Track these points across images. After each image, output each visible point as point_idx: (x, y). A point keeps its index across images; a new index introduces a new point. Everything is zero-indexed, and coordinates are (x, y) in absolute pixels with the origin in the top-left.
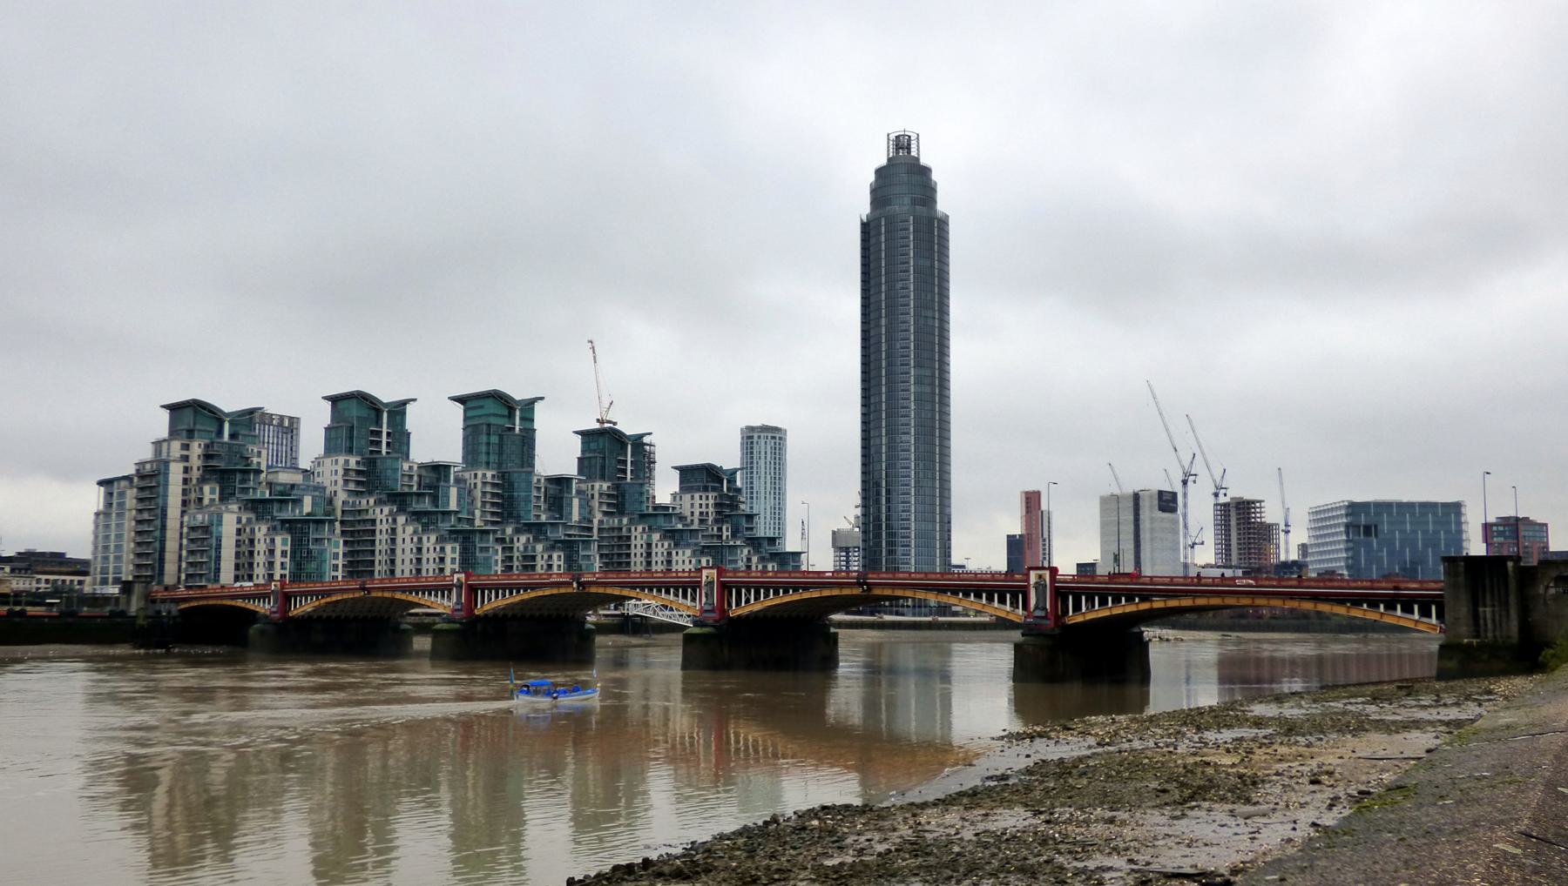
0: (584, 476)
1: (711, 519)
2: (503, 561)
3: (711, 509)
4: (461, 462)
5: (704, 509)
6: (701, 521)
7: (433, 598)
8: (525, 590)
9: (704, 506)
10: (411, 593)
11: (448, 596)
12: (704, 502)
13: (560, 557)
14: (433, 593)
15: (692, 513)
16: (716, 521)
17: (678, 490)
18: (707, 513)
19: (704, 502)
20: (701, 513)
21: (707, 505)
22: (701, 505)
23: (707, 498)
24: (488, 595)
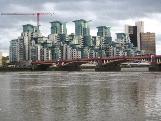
0: (77, 34)
1: (124, 44)
2: (61, 54)
3: (124, 42)
5: (122, 42)
6: (122, 45)
12: (122, 41)
13: (80, 52)
15: (120, 43)
16: (125, 45)
18: (123, 43)
19: (122, 41)
20: (122, 43)
21: (123, 41)
22: (122, 41)
23: (123, 40)
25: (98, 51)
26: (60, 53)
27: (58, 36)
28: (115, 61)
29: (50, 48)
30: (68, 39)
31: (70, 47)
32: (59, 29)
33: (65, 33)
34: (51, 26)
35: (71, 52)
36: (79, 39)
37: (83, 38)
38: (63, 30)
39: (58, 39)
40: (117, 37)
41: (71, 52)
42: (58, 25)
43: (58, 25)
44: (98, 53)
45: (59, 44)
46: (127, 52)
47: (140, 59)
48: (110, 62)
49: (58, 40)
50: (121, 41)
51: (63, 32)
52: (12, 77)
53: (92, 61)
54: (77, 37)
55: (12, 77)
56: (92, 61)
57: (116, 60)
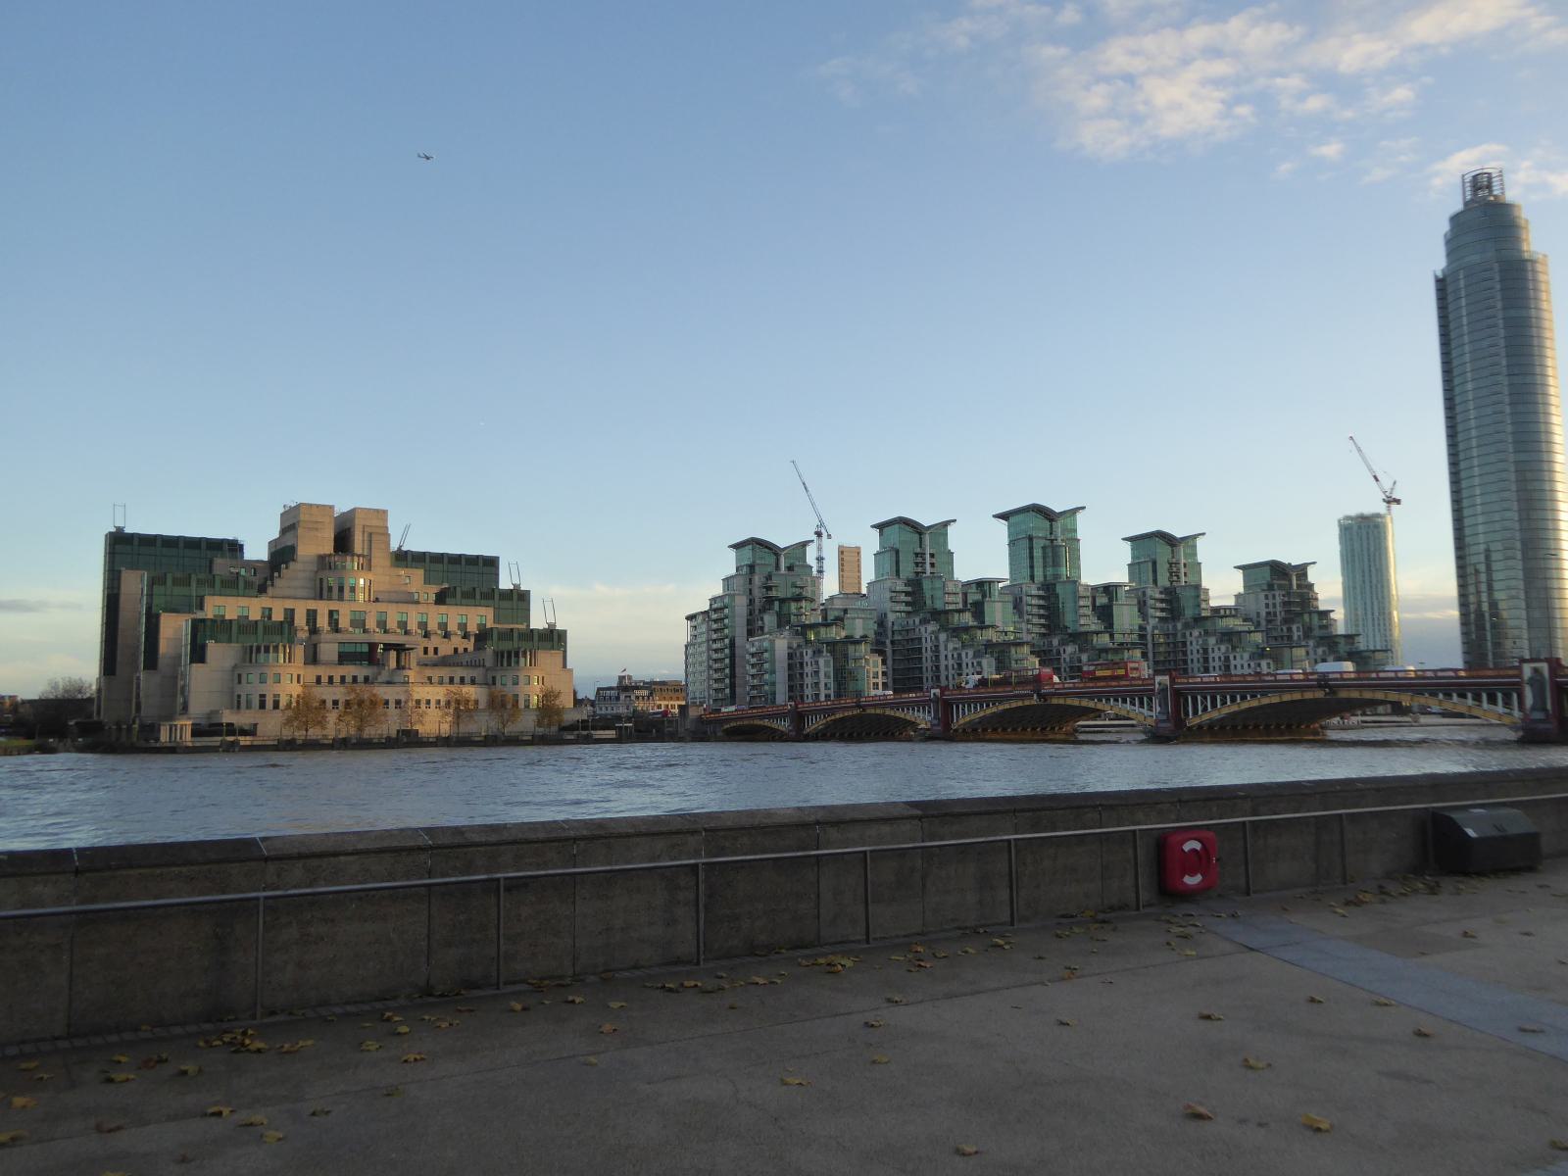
1: (1279, 618)
3: (1278, 609)
4: (1127, 581)
5: (1271, 609)
6: (1269, 622)
7: (1128, 706)
8: (1243, 698)
9: (1271, 606)
10: (1100, 700)
16: (1286, 621)
17: (1242, 590)
18: (1275, 613)
19: (1271, 602)
20: (1268, 613)
21: (1274, 605)
22: (1267, 605)
23: (1274, 597)
24: (1202, 703)
31: (1317, 646)
33: (1192, 580)
34: (1129, 561)
35: (1199, 656)
39: (1162, 610)
45: (1168, 629)
49: (1164, 614)
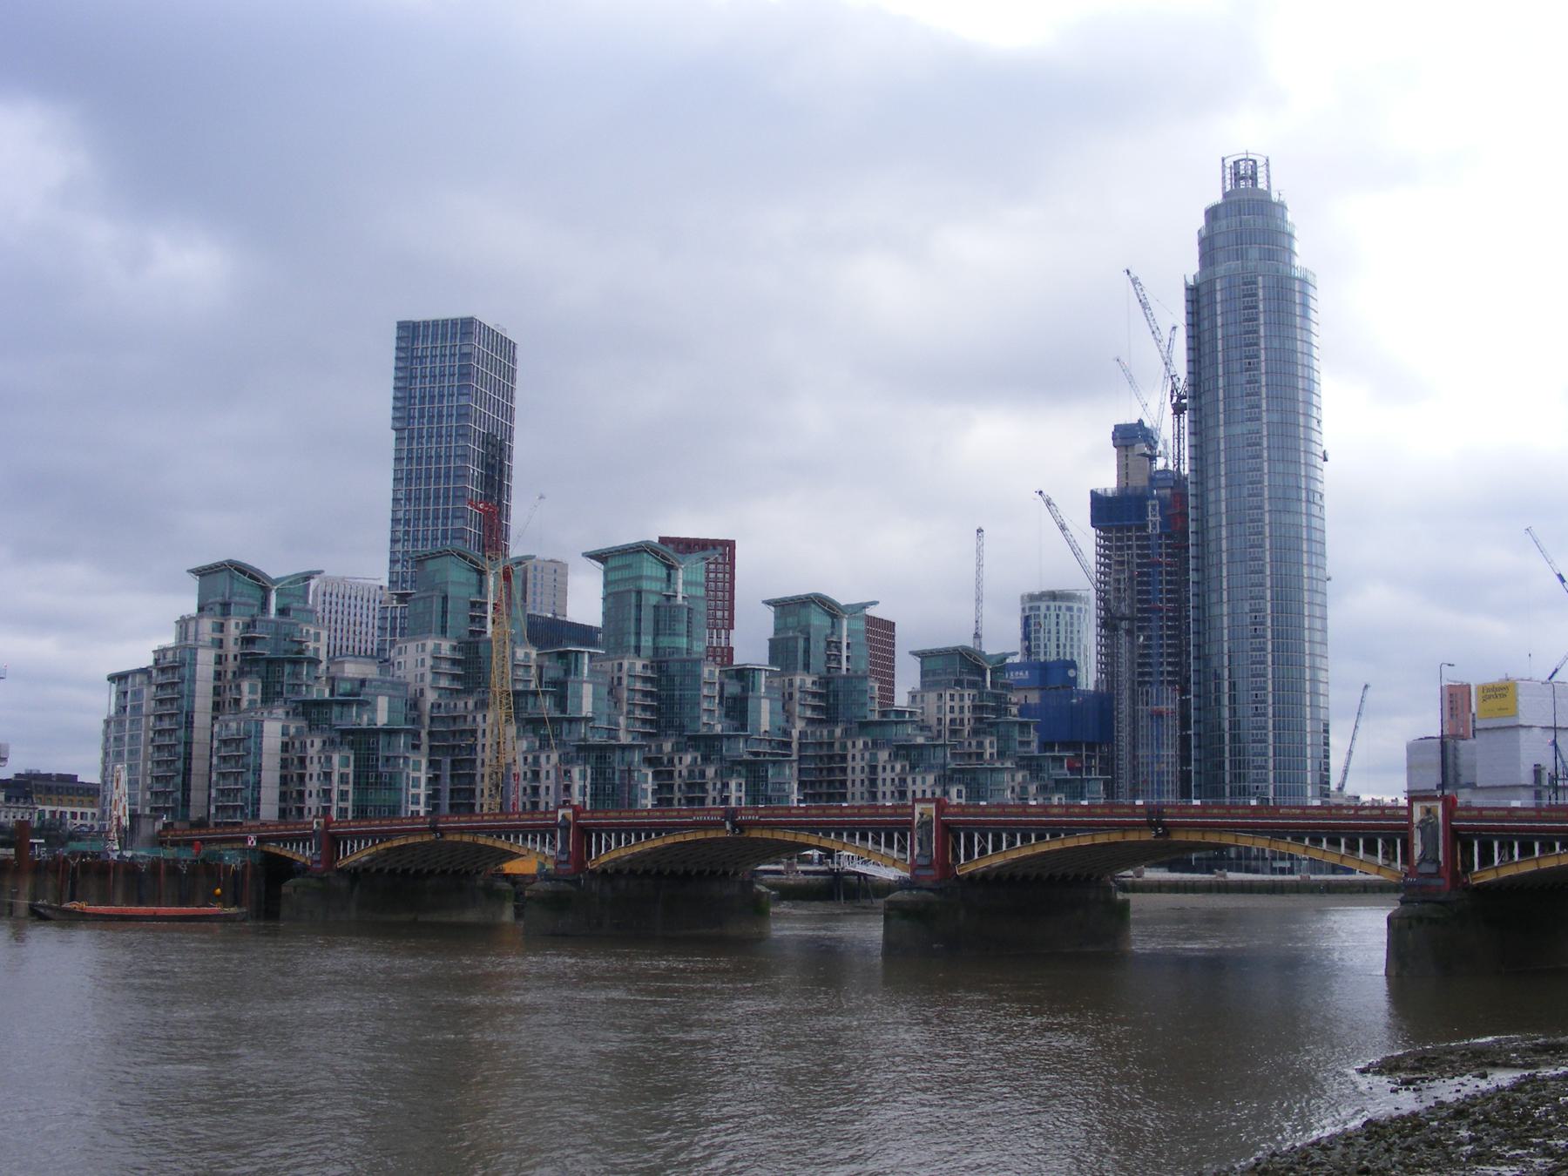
1: (967, 729)
2: (654, 792)
3: (967, 715)
5: (956, 715)
6: (954, 732)
9: (957, 709)
11: (550, 843)
14: (529, 837)
16: (975, 732)
17: (918, 686)
18: (962, 720)
19: (956, 704)
20: (952, 721)
21: (962, 708)
22: (952, 708)
24: (606, 840)
25: (959, 781)
26: (650, 785)
27: (649, 673)
28: (1071, 843)
29: (584, 750)
30: (716, 693)
32: (823, 644)
36: (791, 695)
37: (815, 689)
38: (845, 653)
40: (924, 674)
41: (893, 788)
42: (818, 620)
43: (818, 620)
44: (959, 792)
46: (1063, 796)
47: (1316, 841)
48: (1028, 852)
50: (949, 704)
51: (844, 665)
52: (865, 908)
53: (864, 838)
54: (776, 682)
55: (865, 908)
56: (864, 838)
57: (1085, 840)
